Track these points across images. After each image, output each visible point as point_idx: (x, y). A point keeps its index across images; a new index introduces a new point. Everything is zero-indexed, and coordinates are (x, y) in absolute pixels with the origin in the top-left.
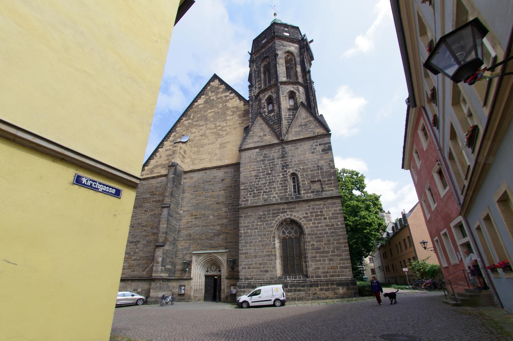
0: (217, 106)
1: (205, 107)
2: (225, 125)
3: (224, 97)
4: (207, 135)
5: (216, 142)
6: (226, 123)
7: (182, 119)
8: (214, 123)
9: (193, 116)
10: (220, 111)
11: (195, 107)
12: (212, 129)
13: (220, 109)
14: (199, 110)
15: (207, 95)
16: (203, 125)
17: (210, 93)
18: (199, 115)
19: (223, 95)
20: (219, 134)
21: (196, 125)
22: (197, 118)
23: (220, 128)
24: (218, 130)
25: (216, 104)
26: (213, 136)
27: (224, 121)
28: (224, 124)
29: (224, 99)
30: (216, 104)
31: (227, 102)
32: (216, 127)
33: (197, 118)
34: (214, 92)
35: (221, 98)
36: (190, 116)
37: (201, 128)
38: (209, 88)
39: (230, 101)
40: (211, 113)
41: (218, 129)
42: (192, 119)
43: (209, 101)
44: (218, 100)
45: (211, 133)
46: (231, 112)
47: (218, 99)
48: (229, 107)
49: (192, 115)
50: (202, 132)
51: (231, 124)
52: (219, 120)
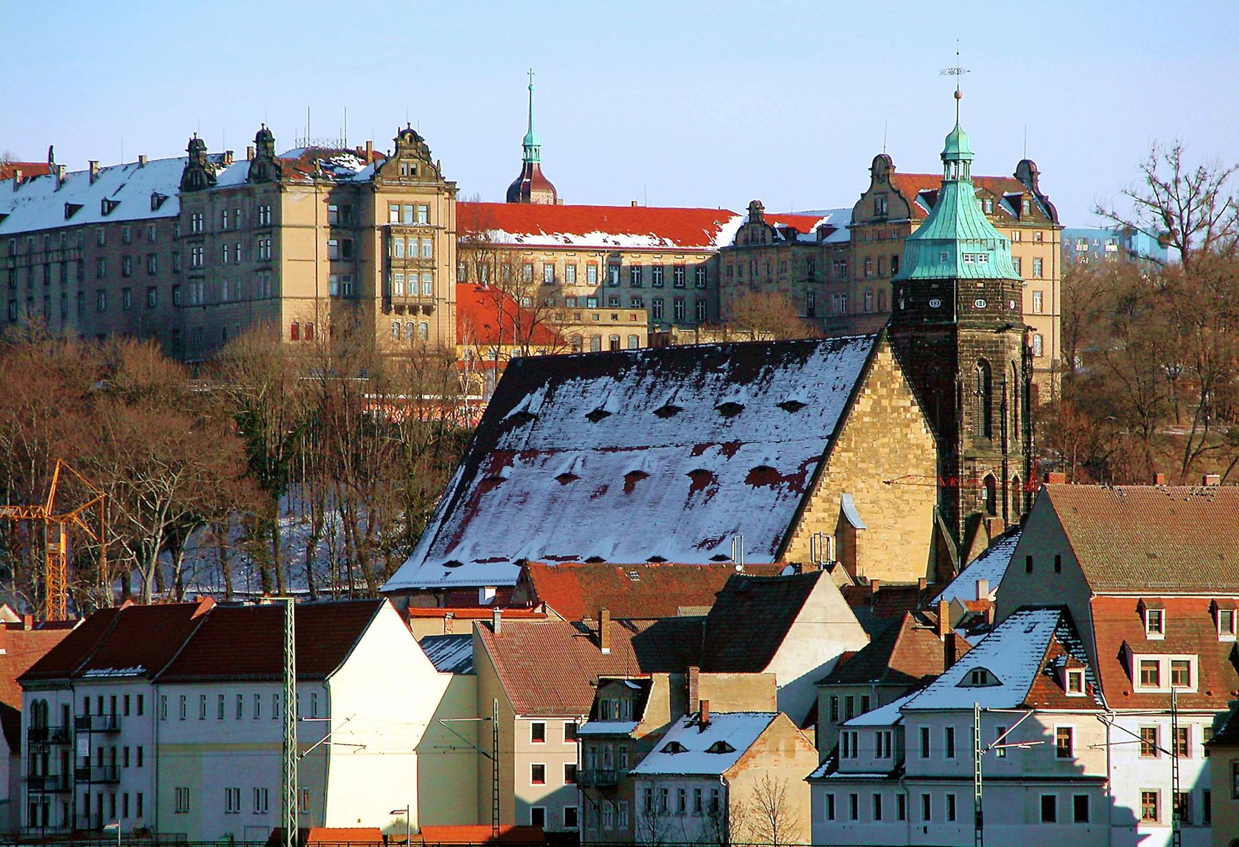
3: (902, 409)
5: (895, 526)
11: (856, 417)
15: (874, 391)
16: (873, 476)
18: (865, 445)
21: (863, 471)
31: (908, 426)
37: (871, 481)
39: (912, 425)
40: (883, 445)
41: (897, 495)
42: (855, 451)
45: (886, 500)
52: (897, 471)
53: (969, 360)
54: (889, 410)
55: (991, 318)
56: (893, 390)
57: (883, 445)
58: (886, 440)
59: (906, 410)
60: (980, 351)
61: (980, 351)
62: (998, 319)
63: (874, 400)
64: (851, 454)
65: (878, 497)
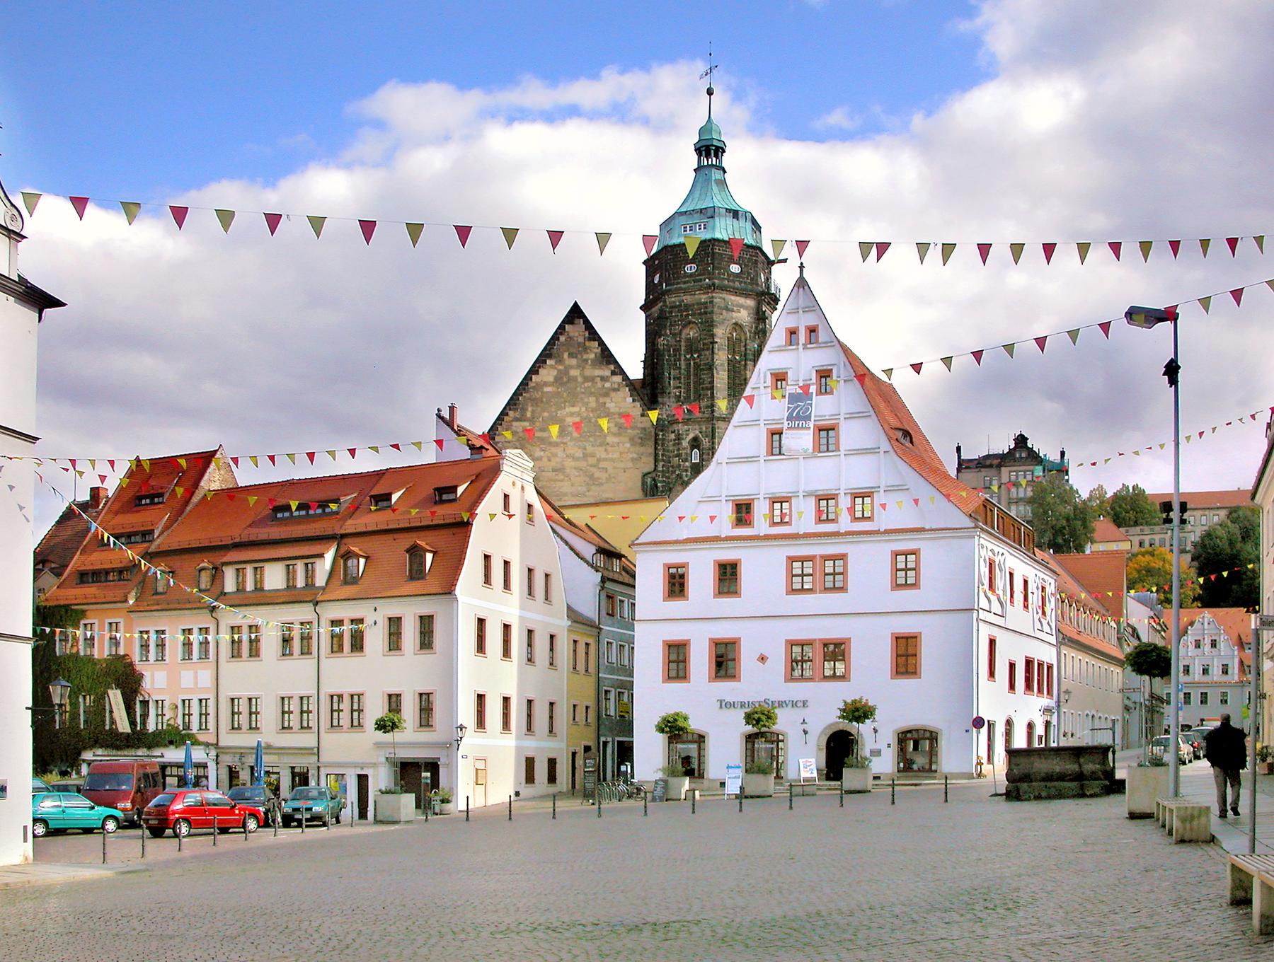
0: (586, 400)
1: (557, 394)
2: (603, 455)
3: (599, 379)
4: (568, 471)
5: (587, 493)
6: (606, 450)
7: (507, 414)
8: (580, 443)
9: (533, 412)
10: (591, 415)
11: (534, 388)
12: (577, 459)
13: (592, 411)
14: (544, 400)
15: (560, 361)
16: (556, 445)
17: (566, 355)
18: (546, 414)
19: (598, 372)
20: (593, 475)
22: (541, 419)
23: (592, 461)
24: (591, 466)
25: (583, 393)
26: (580, 476)
27: (601, 445)
28: (600, 452)
29: (599, 385)
30: (583, 393)
31: (606, 395)
32: (585, 456)
33: (541, 419)
34: (576, 357)
35: (592, 379)
36: (524, 410)
37: (554, 450)
38: (562, 338)
39: (613, 394)
40: (572, 414)
41: (590, 463)
42: (532, 420)
43: (565, 379)
44: (586, 385)
45: (575, 468)
46: (616, 426)
47: (586, 379)
48: (612, 410)
49: (530, 409)
50: (557, 463)
51: (616, 456)
52: (591, 439)
53: (679, 325)
54: (580, 379)
55: (701, 280)
56: (586, 361)
57: (572, 414)
58: (576, 409)
59: (603, 379)
60: (689, 315)
61: (689, 315)
62: (707, 280)
63: (559, 371)
64: (526, 424)
65: (563, 465)
